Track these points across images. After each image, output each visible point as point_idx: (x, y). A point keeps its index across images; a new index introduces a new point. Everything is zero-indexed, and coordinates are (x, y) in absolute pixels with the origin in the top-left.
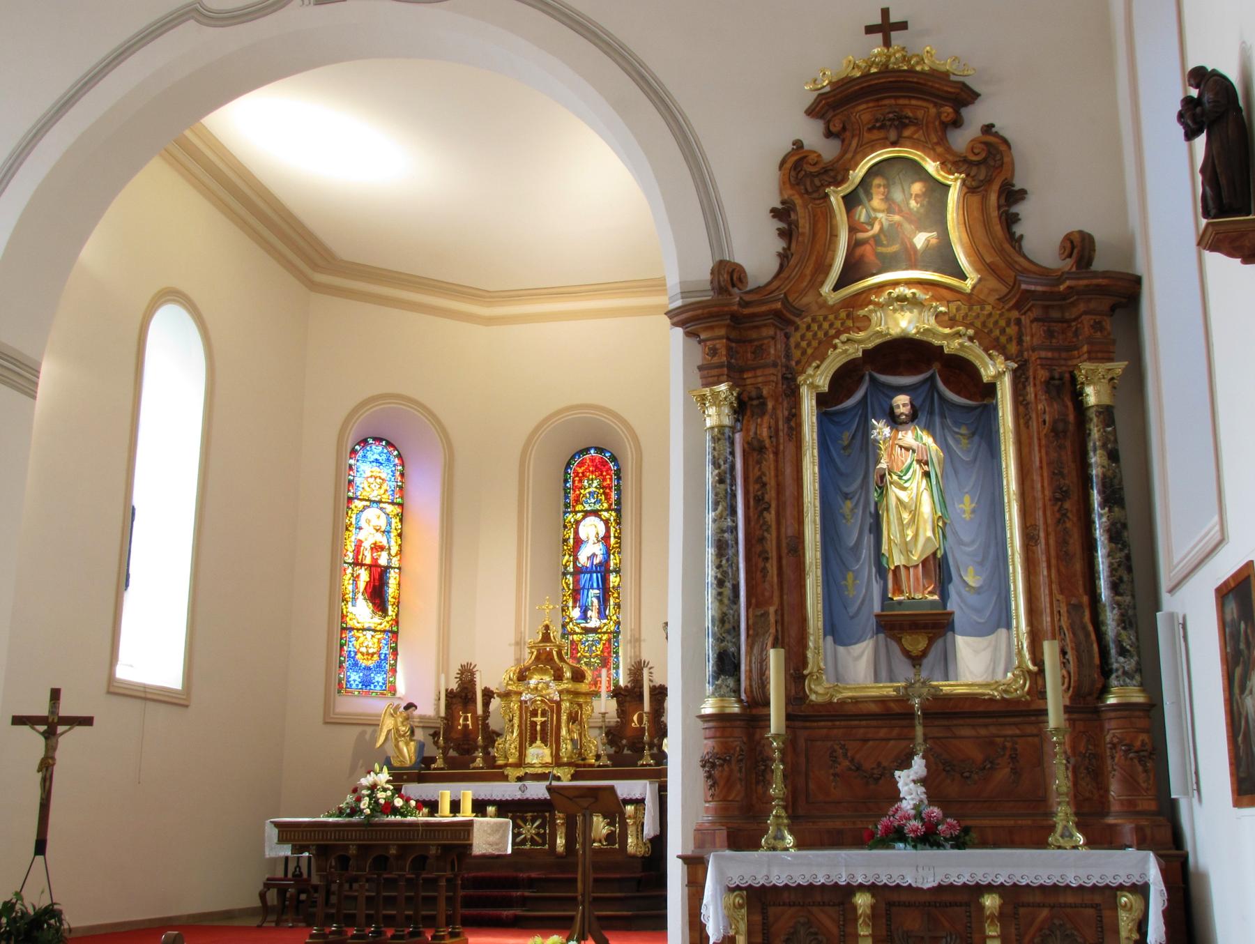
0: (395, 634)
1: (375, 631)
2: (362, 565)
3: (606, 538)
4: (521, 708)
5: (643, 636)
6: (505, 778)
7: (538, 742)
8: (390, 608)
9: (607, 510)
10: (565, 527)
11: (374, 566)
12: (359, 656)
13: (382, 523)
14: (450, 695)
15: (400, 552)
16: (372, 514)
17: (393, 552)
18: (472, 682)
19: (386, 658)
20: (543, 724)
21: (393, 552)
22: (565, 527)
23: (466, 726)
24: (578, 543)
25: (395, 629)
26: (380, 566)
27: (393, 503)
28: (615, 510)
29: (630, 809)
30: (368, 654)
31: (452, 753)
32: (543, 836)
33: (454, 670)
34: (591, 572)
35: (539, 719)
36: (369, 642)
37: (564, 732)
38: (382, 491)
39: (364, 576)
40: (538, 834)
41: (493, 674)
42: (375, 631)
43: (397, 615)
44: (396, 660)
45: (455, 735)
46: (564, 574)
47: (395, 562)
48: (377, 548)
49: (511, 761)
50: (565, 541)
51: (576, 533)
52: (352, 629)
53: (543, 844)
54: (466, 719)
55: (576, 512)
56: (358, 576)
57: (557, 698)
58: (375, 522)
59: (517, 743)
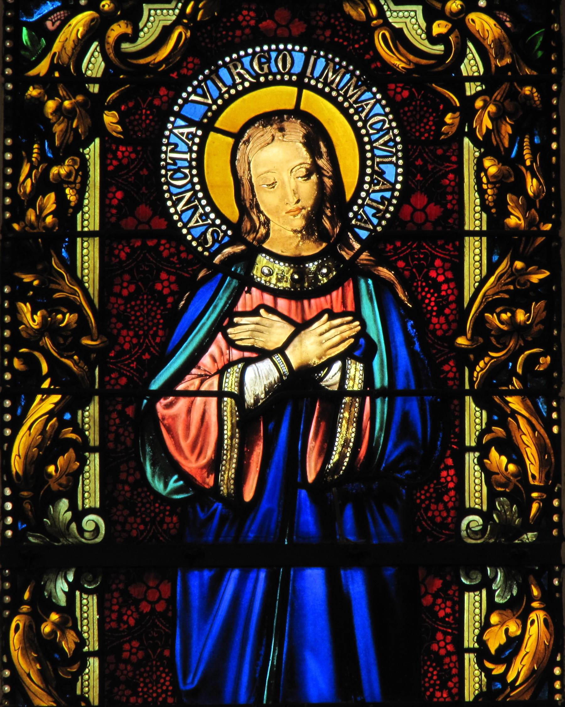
22: (27, 124)
34: (282, 558)
51: (136, 180)
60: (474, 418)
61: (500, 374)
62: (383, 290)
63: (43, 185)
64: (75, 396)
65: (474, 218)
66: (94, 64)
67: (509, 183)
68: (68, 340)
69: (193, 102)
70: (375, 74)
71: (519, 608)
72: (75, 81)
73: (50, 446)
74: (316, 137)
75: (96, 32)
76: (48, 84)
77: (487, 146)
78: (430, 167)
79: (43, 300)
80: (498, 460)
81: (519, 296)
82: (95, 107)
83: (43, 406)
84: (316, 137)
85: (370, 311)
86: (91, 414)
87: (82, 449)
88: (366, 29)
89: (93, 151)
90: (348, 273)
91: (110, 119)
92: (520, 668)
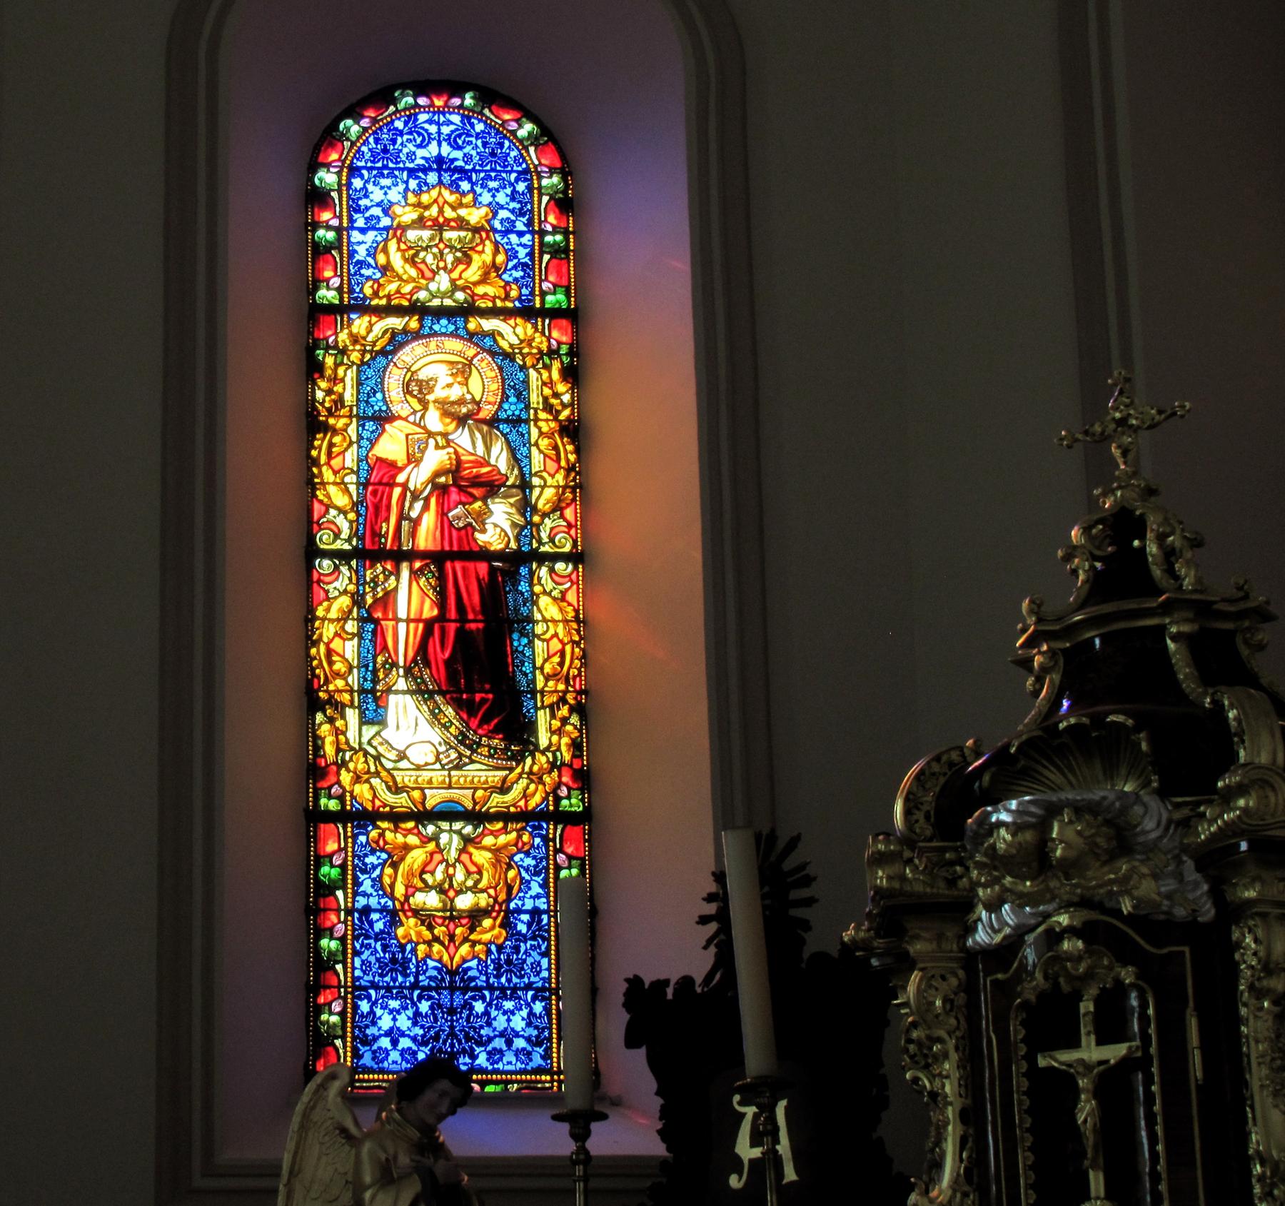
2: (398, 556)
8: (542, 718)
12: (409, 928)
13: (484, 384)
16: (433, 360)
20: (1112, 1083)
21: (544, 497)
26: (485, 555)
27: (527, 312)
30: (452, 916)
38: (473, 274)
39: (411, 598)
42: (477, 817)
47: (554, 534)
48: (465, 484)
52: (364, 818)
56: (387, 600)
58: (446, 388)
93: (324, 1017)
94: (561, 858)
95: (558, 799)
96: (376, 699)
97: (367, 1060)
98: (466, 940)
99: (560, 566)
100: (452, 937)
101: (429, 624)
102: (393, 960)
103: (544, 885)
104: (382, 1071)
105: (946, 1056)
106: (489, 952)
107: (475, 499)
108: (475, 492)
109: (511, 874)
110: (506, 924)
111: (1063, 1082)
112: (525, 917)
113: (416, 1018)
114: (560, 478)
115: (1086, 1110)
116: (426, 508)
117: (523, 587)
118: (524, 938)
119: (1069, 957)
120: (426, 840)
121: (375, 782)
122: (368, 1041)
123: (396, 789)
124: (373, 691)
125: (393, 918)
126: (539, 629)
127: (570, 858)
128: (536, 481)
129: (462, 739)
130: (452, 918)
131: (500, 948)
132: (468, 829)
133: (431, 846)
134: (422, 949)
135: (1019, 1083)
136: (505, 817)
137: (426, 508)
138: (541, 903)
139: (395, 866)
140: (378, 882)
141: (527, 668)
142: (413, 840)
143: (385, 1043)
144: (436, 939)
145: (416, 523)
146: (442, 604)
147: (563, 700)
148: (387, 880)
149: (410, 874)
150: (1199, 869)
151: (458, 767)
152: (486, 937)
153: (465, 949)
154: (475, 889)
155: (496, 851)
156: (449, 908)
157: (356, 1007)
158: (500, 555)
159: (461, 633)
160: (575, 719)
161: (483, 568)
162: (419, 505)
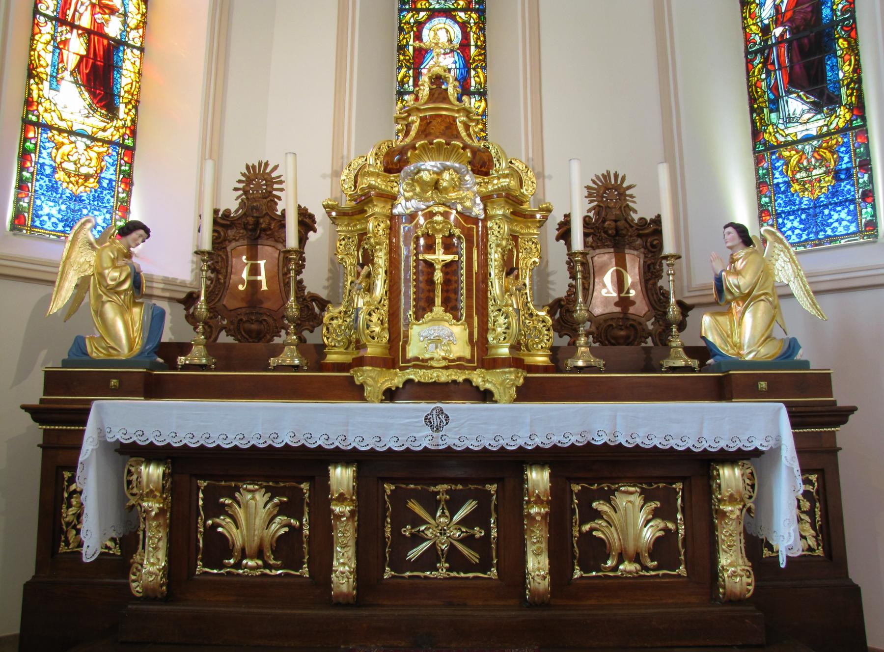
0: (130, 151)
1: (92, 138)
2: (73, 26)
3: (464, 45)
4: (392, 230)
5: (546, 173)
6: (357, 392)
7: (438, 310)
8: (122, 107)
9: (462, 10)
10: (401, 29)
11: (94, 33)
12: (60, 175)
14: (223, 224)
15: (144, 23)
17: (133, 22)
18: (271, 199)
19: (111, 188)
20: (450, 268)
21: (133, 22)
23: (254, 285)
24: (421, 54)
25: (129, 142)
26: (106, 37)
28: (477, 11)
29: (730, 477)
31: (224, 338)
32: (481, 545)
33: (233, 174)
35: (440, 257)
36: (81, 156)
37: (496, 287)
39: (77, 46)
40: (468, 541)
41: (307, 186)
42: (92, 138)
43: (133, 121)
44: (129, 193)
45: (229, 302)
46: (401, 94)
47: (134, 37)
49: (372, 351)
50: (401, 49)
52: (48, 127)
53: (484, 566)
54: (254, 271)
55: (418, 11)
56: (65, 42)
57: (478, 211)
59: (384, 311)
60: (473, 73)
61: (477, 67)
62: (458, 53)
63: (404, 38)
64: (409, 69)
65: (472, 43)
66: (412, 21)
67: (478, 38)
68: (408, 61)
69: (428, 26)
70: (457, 22)
71: (480, 101)
72: (409, 23)
73: (405, 76)
74: (447, 31)
75: (413, 16)
76: (405, 24)
77: (475, 33)
78: (466, 36)
79: (404, 55)
80: (477, 79)
81: (480, 55)
82: (412, 27)
83: (404, 70)
84: (447, 31)
85: (456, 56)
86: (411, 72)
87: (409, 77)
88: (455, 16)
89: (412, 33)
90: (452, 51)
91: (415, 29)
92: (480, 111)
93: (21, 203)
94: (123, 162)
95: (124, 140)
96: (57, 81)
97: (37, 223)
98: (83, 185)
99: (135, 51)
100: (77, 182)
101: (82, 57)
102: (53, 187)
103: (115, 171)
104: (43, 229)
105: (381, 250)
106: (91, 191)
107: (105, 13)
108: (107, 11)
109: (103, 163)
110: (99, 182)
111: (430, 265)
112: (107, 181)
113: (60, 211)
114: (140, 16)
115: (438, 276)
116: (86, 10)
117: (121, 54)
118: (106, 189)
119: (436, 222)
120: (72, 143)
121: (53, 113)
122: (38, 216)
123: (62, 119)
124: (56, 77)
125: (54, 170)
126: (124, 72)
127: (126, 162)
128: (129, 15)
129: (90, 106)
130: (78, 175)
131: (96, 191)
132: (88, 142)
133: (73, 145)
134: (65, 185)
135: (412, 264)
136: (103, 141)
137: (86, 10)
138: (114, 178)
139: (57, 149)
140: (50, 154)
141: (118, 86)
142: (66, 141)
143: (45, 218)
144: (71, 182)
145: (81, 15)
146: (88, 50)
147: (130, 102)
148: (53, 155)
149: (63, 155)
150: (481, 200)
151: (87, 117)
152: (91, 186)
153: (82, 188)
154: (88, 166)
155: (99, 154)
156: (77, 170)
157: (34, 202)
158: (113, 39)
159: (94, 64)
160: (133, 111)
161: (105, 42)
162: (84, 8)
